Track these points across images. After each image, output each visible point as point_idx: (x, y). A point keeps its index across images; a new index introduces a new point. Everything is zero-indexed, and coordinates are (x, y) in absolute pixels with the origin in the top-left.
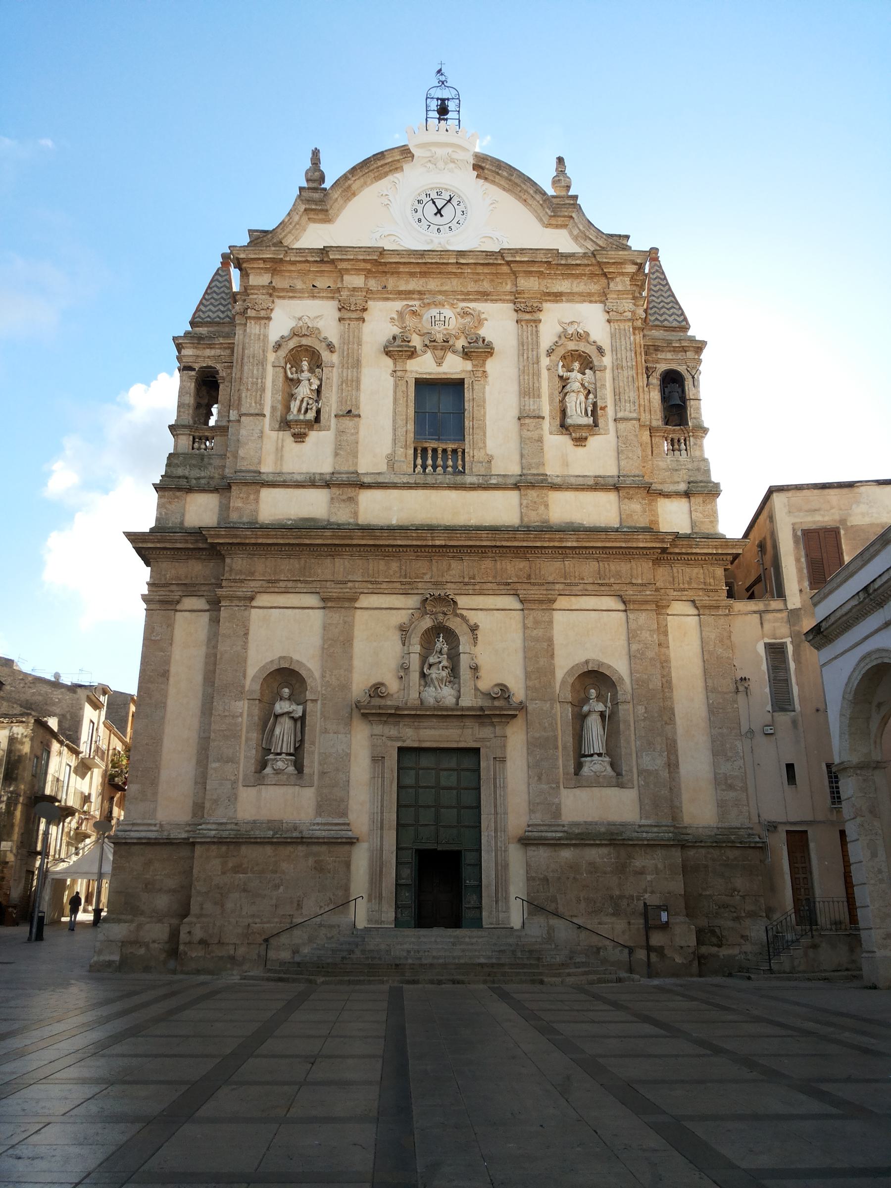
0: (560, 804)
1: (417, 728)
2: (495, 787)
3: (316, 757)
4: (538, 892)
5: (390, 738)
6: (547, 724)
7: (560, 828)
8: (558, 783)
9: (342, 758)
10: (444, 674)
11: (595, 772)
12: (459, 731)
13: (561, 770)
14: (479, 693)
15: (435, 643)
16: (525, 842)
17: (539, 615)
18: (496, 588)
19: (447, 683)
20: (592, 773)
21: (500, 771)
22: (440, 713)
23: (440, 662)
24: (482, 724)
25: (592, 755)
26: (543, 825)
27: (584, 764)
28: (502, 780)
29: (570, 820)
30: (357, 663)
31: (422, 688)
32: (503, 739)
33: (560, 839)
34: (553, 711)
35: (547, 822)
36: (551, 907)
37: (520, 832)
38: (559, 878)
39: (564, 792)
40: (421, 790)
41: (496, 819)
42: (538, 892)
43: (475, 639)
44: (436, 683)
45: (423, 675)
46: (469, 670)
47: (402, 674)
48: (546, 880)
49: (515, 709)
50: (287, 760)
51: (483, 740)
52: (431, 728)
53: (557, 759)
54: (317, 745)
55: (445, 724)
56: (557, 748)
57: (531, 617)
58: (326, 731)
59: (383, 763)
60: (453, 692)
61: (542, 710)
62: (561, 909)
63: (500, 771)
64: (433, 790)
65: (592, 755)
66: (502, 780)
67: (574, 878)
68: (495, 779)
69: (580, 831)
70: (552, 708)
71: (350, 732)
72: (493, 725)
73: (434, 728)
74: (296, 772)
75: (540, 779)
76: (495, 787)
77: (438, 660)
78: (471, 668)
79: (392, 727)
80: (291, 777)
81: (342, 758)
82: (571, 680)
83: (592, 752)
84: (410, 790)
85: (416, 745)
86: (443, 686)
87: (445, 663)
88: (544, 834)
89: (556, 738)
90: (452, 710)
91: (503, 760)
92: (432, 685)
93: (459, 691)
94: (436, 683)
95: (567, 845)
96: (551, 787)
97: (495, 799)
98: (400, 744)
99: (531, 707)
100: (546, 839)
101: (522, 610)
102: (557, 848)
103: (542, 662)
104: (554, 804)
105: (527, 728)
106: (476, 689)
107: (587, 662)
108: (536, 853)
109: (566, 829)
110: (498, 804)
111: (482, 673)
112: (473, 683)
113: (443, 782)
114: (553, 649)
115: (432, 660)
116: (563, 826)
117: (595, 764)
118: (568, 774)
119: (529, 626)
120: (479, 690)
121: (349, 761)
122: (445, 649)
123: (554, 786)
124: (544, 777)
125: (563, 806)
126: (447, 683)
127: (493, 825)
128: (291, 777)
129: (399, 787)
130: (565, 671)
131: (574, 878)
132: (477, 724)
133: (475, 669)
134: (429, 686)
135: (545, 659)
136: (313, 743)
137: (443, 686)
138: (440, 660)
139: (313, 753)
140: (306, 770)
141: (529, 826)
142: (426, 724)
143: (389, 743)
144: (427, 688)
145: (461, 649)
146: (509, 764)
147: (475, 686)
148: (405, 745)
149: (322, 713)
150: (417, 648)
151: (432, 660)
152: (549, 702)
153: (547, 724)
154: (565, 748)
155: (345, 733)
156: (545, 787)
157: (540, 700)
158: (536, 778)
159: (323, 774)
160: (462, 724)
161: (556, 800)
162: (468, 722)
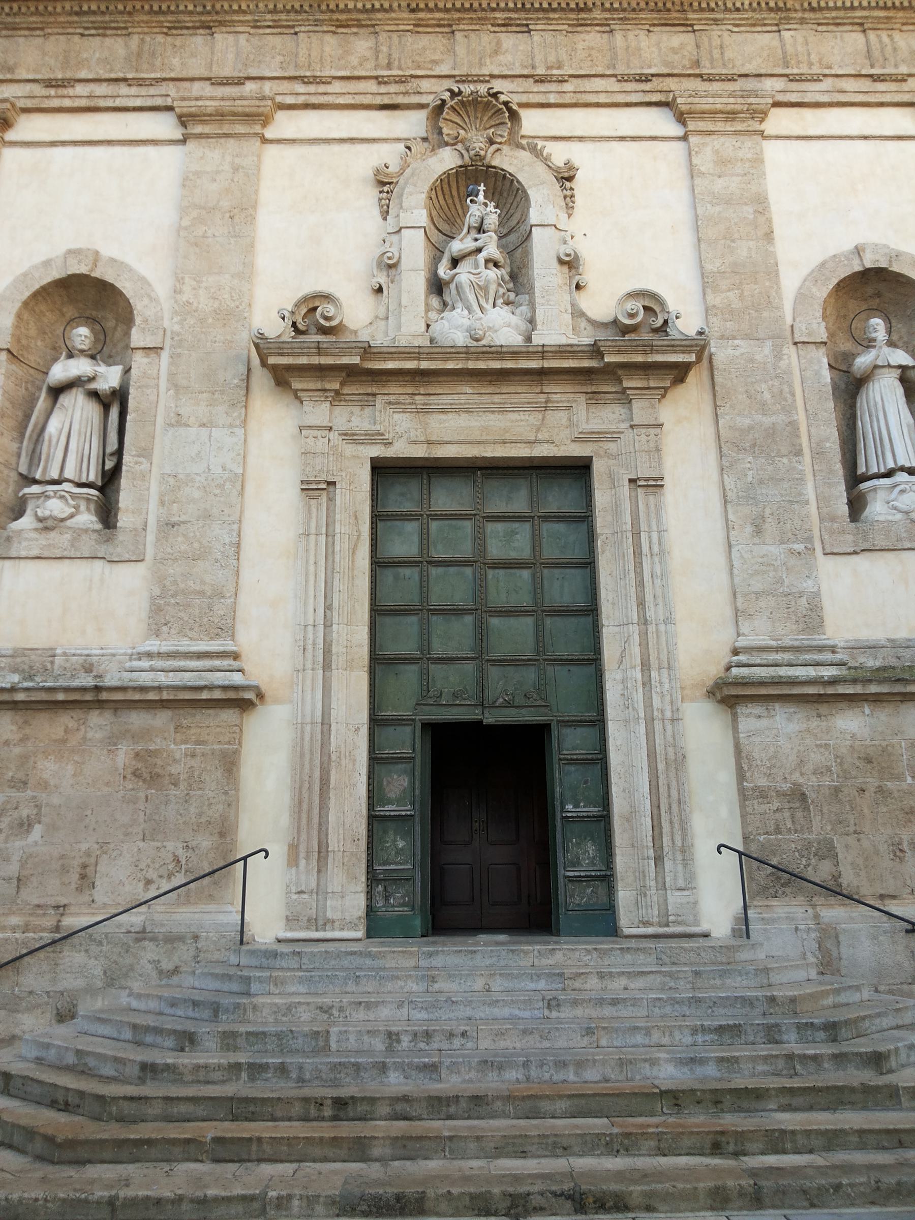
0: (817, 594)
1: (425, 411)
2: (638, 553)
3: (154, 488)
4: (778, 830)
5: (350, 437)
6: (767, 396)
7: (827, 656)
8: (810, 539)
9: (221, 486)
10: (492, 274)
11: (907, 513)
12: (534, 418)
13: (813, 508)
14: (583, 324)
15: (465, 210)
16: (734, 691)
17: (726, 145)
18: (616, 87)
19: (500, 301)
20: (898, 516)
21: (648, 515)
22: (481, 365)
23: (479, 250)
24: (594, 398)
25: (889, 474)
26: (777, 649)
27: (869, 497)
28: (655, 536)
29: (849, 636)
30: (263, 261)
31: (433, 315)
32: (652, 431)
33: (833, 682)
34: (783, 364)
35: (787, 642)
36: (822, 871)
37: (714, 671)
38: (836, 791)
39: (826, 566)
40: (434, 571)
41: (644, 635)
42: (778, 830)
43: (569, 200)
44: (471, 298)
45: (437, 287)
46: (555, 262)
47: (382, 279)
48: (799, 796)
49: (686, 349)
50: (74, 496)
51: (598, 437)
52: (458, 410)
53: (802, 480)
54: (155, 461)
55: (497, 399)
56: (799, 453)
57: (708, 151)
58: (179, 421)
59: (331, 500)
60: (515, 320)
61: (752, 360)
62: (848, 879)
63: (648, 515)
64: (468, 571)
65: (889, 474)
66: (655, 536)
67: (880, 790)
68: (636, 534)
69: (878, 664)
70: (778, 356)
71: (245, 422)
72: (623, 397)
73: (467, 411)
74: (99, 526)
75: (758, 530)
76: (638, 553)
77: (472, 245)
78: (561, 262)
79: (357, 410)
80: (84, 537)
81: (221, 486)
82: (823, 291)
83: (891, 465)
84: (406, 572)
85: (419, 452)
86: (488, 306)
87: (492, 250)
88: (783, 672)
89: (793, 425)
90: (515, 354)
91: (655, 485)
92: (459, 305)
93: (532, 321)
94: (471, 298)
95: (852, 699)
96: (792, 552)
97: (641, 584)
98: (377, 451)
99: (721, 352)
100: (793, 682)
101: (684, 138)
102: (824, 709)
103: (744, 250)
104: (801, 594)
105: (716, 407)
106: (578, 313)
107: (858, 251)
108: (764, 723)
109: (839, 657)
110: (649, 597)
111: (590, 274)
112: (567, 297)
113: (495, 550)
114: (769, 221)
115: (457, 246)
116: (833, 649)
117: (903, 491)
118: (833, 519)
119: (703, 169)
120: (582, 314)
121: (242, 493)
122: (492, 220)
123: (799, 547)
124: (770, 526)
125: (826, 603)
126: (500, 301)
127: (636, 650)
128: (84, 537)
129: (379, 564)
130: (805, 271)
131: (880, 790)
132: (583, 398)
133: (570, 263)
134: (454, 308)
135: (751, 243)
136: (146, 453)
137: (488, 306)
138: (479, 244)
139: (144, 477)
140: (124, 520)
141: (736, 652)
142: (446, 400)
143: (349, 450)
144: (445, 314)
145: (534, 216)
146: (671, 495)
147: (572, 305)
148: (390, 452)
149: (172, 376)
150: (421, 217)
151: (457, 246)
152: (769, 343)
153: (767, 396)
154: (818, 454)
155: (231, 426)
156: (775, 550)
157: (747, 337)
158: (749, 529)
159: (169, 526)
160: (542, 398)
161: (809, 585)
162: (559, 392)
